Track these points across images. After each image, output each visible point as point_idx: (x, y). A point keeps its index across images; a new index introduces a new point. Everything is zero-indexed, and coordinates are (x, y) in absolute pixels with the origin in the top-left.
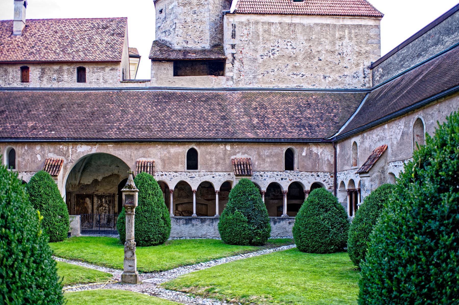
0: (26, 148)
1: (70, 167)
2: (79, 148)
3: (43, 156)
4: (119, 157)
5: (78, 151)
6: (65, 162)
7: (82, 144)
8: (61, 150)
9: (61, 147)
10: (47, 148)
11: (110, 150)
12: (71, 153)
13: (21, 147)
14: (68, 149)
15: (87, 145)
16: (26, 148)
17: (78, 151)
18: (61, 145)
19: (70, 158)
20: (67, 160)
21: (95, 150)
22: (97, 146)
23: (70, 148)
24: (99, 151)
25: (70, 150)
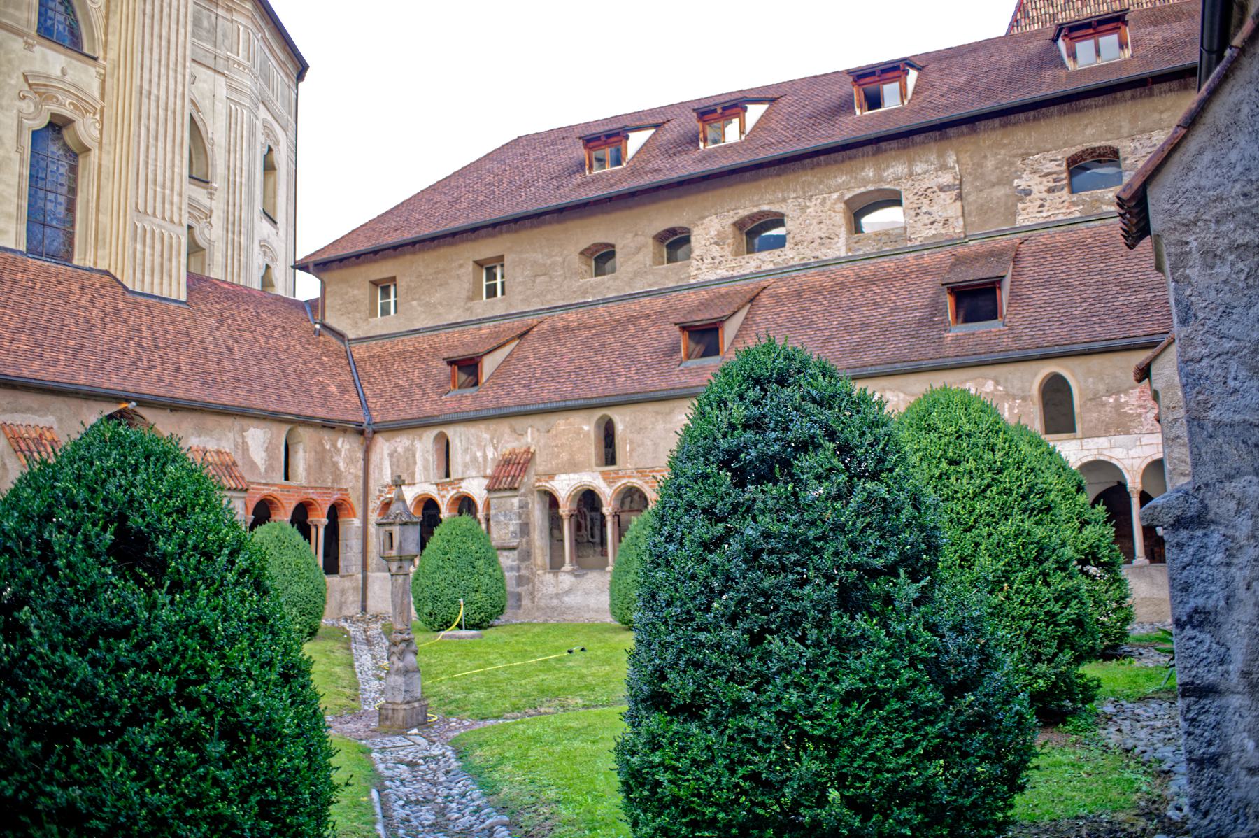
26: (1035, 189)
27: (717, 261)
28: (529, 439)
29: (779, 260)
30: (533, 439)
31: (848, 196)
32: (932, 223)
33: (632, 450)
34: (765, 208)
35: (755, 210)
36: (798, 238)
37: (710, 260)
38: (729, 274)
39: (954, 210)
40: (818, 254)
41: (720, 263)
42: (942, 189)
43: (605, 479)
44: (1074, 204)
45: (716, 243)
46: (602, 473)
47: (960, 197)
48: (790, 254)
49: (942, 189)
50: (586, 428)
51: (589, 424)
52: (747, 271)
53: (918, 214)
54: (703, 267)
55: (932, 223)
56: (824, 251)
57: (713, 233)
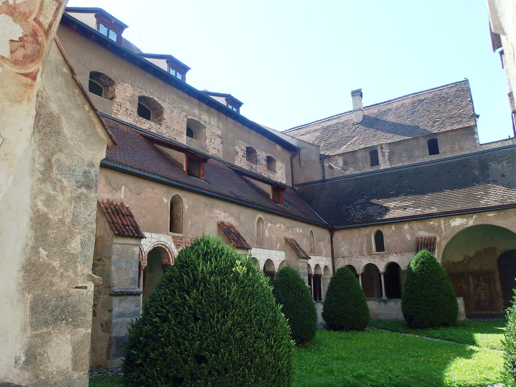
0: (393, 228)
1: (444, 243)
2: (452, 222)
3: (412, 235)
4: (504, 227)
5: (452, 226)
6: (438, 239)
7: (456, 218)
8: (432, 227)
9: (432, 223)
10: (415, 225)
11: (491, 219)
12: (443, 228)
13: (388, 229)
14: (440, 224)
15: (462, 218)
16: (393, 228)
17: (452, 226)
18: (431, 221)
19: (444, 234)
20: (441, 236)
21: (471, 222)
22: (474, 217)
23: (442, 223)
24: (477, 223)
25: (442, 226)
26: (240, 153)
27: (129, 112)
28: (122, 196)
29: (159, 130)
30: (125, 196)
31: (189, 117)
32: (215, 148)
33: (192, 225)
34: (156, 99)
35: (151, 97)
36: (169, 125)
37: (124, 109)
38: (135, 124)
39: (220, 147)
40: (176, 137)
41: (130, 114)
42: (218, 136)
43: (174, 242)
44: (247, 165)
45: (129, 101)
46: (173, 237)
47: (222, 143)
48: (165, 131)
49: (218, 136)
50: (165, 200)
51: (167, 198)
52: (144, 128)
53: (211, 142)
54: (121, 111)
55: (215, 148)
56: (178, 138)
57: (128, 94)
